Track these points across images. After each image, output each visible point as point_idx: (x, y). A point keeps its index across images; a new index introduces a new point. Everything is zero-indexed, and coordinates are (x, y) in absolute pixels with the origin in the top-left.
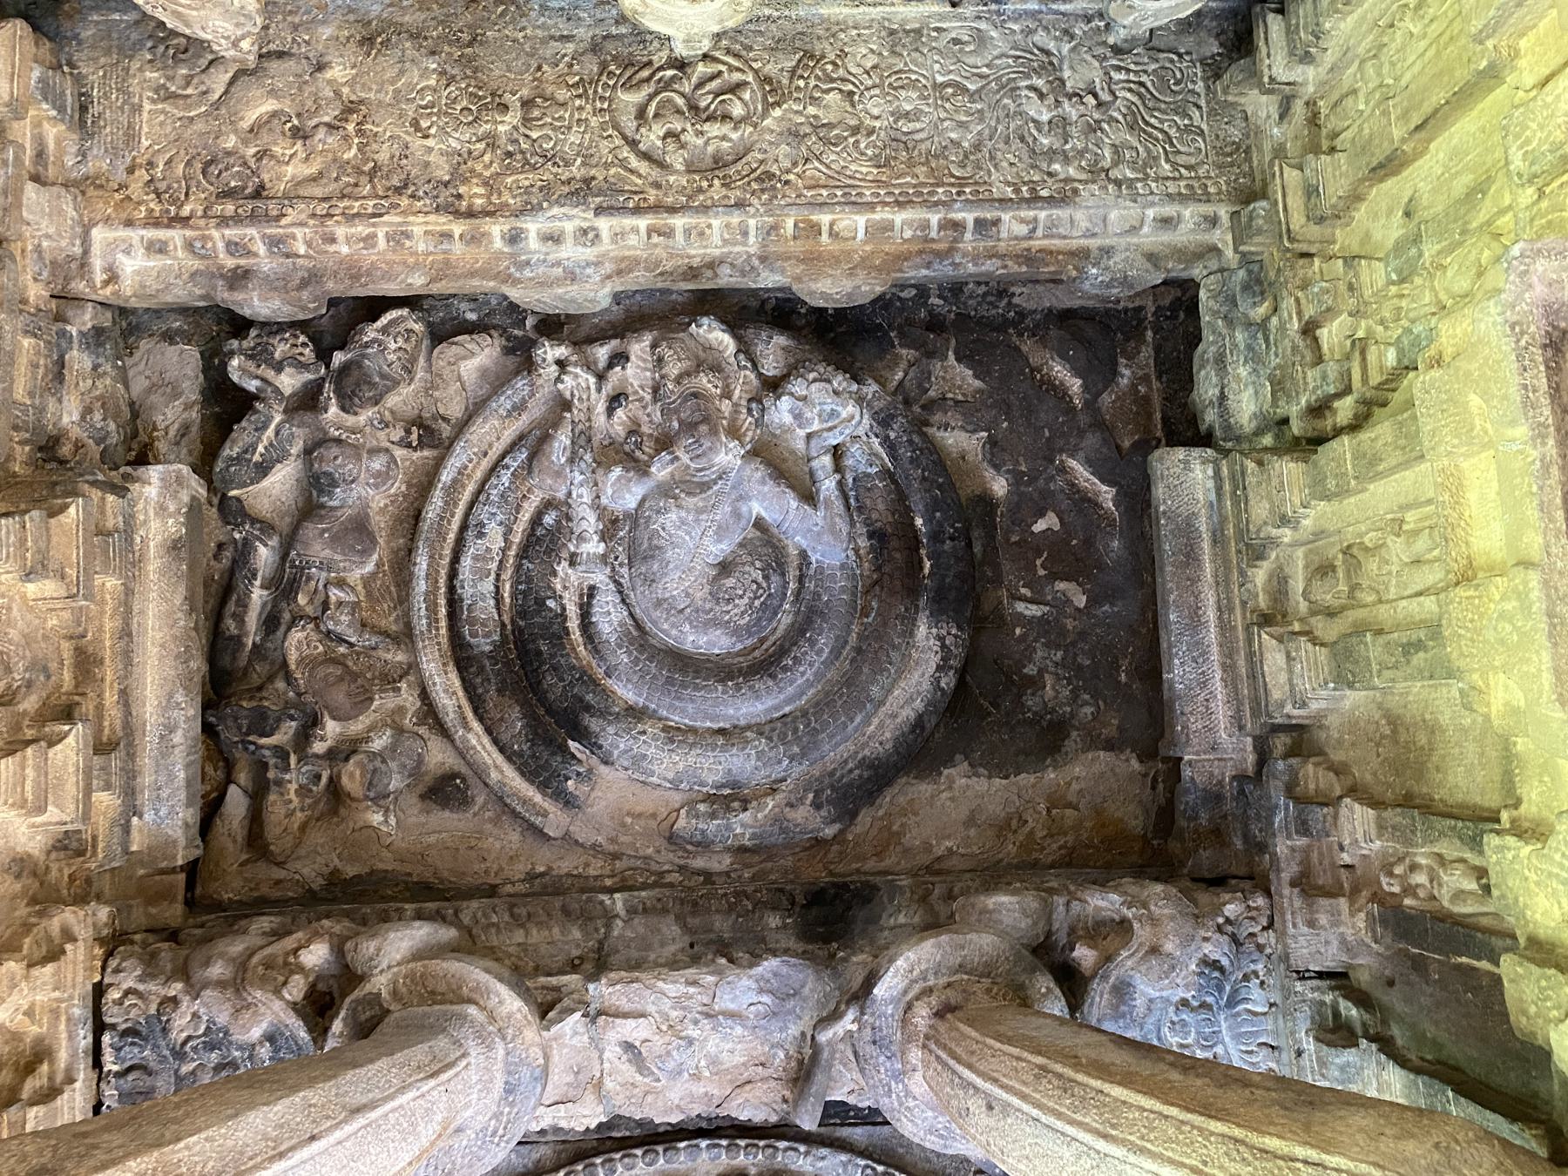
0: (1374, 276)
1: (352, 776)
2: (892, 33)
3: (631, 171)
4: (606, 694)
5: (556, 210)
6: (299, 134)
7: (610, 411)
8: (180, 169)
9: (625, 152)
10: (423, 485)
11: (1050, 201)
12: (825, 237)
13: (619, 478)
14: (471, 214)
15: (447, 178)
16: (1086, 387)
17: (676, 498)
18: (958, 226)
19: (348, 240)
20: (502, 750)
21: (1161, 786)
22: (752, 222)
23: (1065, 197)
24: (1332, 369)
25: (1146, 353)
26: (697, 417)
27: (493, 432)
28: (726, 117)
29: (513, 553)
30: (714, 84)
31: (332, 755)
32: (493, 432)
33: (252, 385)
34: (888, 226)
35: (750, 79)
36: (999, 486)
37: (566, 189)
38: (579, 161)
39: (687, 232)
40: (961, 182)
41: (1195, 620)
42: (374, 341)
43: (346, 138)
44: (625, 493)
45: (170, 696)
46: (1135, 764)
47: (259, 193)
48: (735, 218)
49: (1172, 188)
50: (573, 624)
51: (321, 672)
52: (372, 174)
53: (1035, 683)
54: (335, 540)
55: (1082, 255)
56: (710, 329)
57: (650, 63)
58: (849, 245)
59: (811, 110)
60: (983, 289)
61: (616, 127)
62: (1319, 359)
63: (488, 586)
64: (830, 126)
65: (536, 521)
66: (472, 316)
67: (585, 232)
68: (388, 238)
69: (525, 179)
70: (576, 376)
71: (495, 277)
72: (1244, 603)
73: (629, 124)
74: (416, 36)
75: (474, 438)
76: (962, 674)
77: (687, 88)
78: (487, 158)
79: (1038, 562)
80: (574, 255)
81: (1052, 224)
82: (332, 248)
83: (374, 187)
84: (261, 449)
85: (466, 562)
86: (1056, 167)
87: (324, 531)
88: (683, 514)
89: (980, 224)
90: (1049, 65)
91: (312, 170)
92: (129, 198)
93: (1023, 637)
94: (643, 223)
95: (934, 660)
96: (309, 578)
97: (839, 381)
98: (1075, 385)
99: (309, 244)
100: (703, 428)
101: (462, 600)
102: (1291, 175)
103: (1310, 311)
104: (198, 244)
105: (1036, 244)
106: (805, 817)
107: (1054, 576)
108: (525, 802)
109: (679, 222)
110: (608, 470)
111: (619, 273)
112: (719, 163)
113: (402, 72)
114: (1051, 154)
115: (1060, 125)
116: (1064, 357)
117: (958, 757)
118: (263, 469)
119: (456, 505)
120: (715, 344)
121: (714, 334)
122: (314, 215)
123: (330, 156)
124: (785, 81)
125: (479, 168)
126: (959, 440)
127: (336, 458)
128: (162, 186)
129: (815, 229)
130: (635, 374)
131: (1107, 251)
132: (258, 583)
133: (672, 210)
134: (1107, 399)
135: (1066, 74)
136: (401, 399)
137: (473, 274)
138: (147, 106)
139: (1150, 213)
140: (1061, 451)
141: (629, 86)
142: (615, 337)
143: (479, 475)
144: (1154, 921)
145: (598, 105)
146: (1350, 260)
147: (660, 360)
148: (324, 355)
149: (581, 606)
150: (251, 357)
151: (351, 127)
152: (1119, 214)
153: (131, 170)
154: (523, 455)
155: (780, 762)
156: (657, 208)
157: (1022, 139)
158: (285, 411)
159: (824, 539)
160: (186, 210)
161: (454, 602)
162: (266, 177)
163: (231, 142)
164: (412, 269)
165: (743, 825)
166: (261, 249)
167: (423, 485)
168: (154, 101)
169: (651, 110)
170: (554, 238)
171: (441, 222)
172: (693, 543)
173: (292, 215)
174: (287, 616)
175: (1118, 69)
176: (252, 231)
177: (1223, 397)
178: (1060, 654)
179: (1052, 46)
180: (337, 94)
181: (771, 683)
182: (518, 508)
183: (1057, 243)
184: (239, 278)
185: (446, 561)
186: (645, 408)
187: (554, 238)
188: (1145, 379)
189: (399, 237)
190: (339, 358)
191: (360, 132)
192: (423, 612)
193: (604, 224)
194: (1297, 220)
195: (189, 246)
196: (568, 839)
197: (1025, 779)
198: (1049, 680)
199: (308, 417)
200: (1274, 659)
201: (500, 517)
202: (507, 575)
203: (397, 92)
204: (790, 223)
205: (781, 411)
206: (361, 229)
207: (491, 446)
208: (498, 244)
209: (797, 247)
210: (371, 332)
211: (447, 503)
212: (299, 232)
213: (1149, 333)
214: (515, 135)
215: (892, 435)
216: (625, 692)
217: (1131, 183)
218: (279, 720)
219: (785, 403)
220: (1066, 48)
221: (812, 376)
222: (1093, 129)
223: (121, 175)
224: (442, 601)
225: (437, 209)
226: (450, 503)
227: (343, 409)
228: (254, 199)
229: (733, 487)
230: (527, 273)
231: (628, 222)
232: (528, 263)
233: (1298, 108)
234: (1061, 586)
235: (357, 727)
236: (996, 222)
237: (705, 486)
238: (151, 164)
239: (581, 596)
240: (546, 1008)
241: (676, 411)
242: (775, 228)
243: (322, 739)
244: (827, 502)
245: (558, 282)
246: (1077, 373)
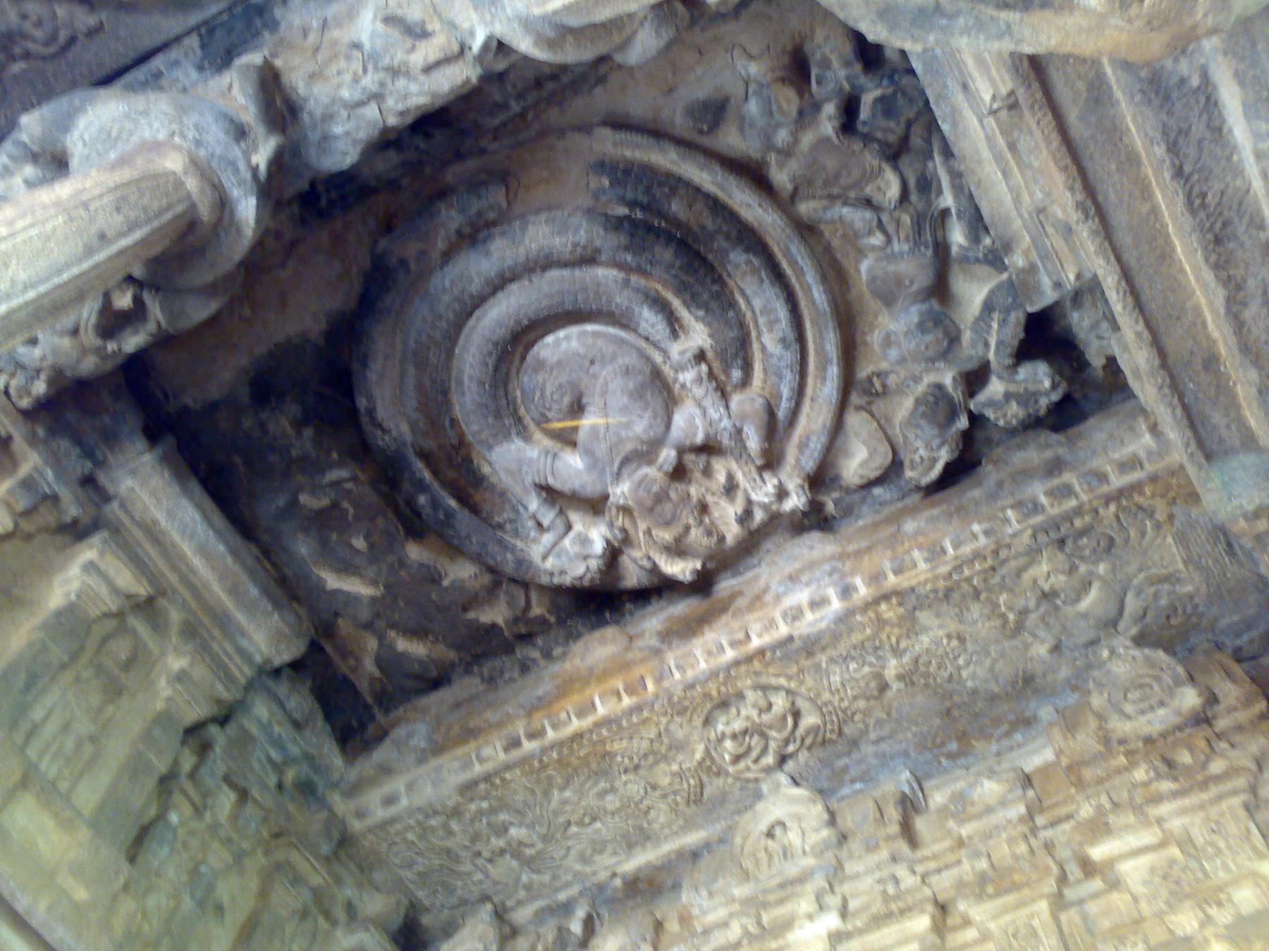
0: (218, 857)
1: (789, 101)
2: (648, 838)
3: (778, 675)
4: (620, 266)
5: (823, 625)
6: (1047, 596)
7: (730, 477)
8: (1132, 533)
9: (793, 685)
10: (849, 352)
11: (475, 783)
12: (621, 687)
13: (695, 434)
14: (886, 597)
15: (918, 613)
16: (392, 647)
17: (643, 442)
18: (532, 736)
19: (975, 536)
20: (679, 179)
21: (162, 397)
22: (677, 675)
23: (468, 789)
24: (210, 782)
25: (364, 687)
26: (658, 509)
27: (813, 420)
28: (734, 737)
29: (754, 334)
30: (754, 754)
31: (817, 107)
32: (813, 420)
33: (1024, 371)
34: (581, 714)
35: (731, 769)
36: (415, 552)
37: (823, 642)
38: (824, 665)
39: (721, 649)
40: (544, 767)
41: (203, 551)
42: (939, 447)
43: (1011, 608)
44: (690, 421)
45: (955, 124)
46: (188, 400)
47: (1062, 542)
48: (690, 674)
49: (398, 826)
50: (676, 303)
51: (856, 174)
52: (977, 594)
53: (299, 425)
54: (899, 281)
55: (437, 749)
56: (683, 572)
57: (809, 748)
58: (604, 686)
59: (675, 767)
60: (507, 676)
61: (810, 699)
62: (227, 779)
63: (758, 303)
64: (656, 763)
65: (747, 368)
66: (877, 491)
67: (795, 618)
68: (944, 551)
69: (856, 638)
70: (766, 494)
71: (848, 556)
72: (175, 591)
73: (802, 704)
74: (993, 698)
75: (825, 408)
76: (355, 411)
77: (773, 745)
78: (894, 640)
79: (351, 511)
80: (798, 594)
81: (467, 765)
82: (986, 525)
83: (971, 585)
84: (995, 325)
85: (782, 313)
86: (485, 805)
87: (912, 282)
88: (631, 434)
89: (516, 743)
90: (529, 864)
91: (1027, 577)
92: (1163, 496)
93: (329, 452)
94: (756, 642)
95: (381, 413)
96: (907, 239)
97: (567, 580)
98: (402, 645)
99: (1007, 520)
100: (649, 503)
101: (772, 284)
102: (316, 880)
103: (249, 809)
104: (1095, 483)
105: (473, 745)
106: (411, 249)
107: (335, 505)
108: (637, 146)
109: (730, 654)
110: (707, 436)
111: (758, 598)
112: (724, 705)
113: (991, 669)
114: (493, 811)
115: (503, 830)
116: (420, 662)
117: (321, 342)
118: (988, 307)
119: (816, 352)
120: (677, 560)
121: (681, 569)
122: (1009, 546)
123: (1017, 590)
124: (705, 778)
125: (896, 631)
126: (462, 572)
127: (927, 348)
128: (1140, 515)
129: (630, 691)
130: (727, 515)
131: (421, 760)
132: (953, 211)
133: (737, 663)
134: (372, 644)
135: (515, 864)
136: (903, 407)
137: (869, 549)
138: (1181, 566)
139: (404, 802)
140: (383, 597)
141: (815, 730)
142: (758, 531)
143: (810, 381)
144: (84, 351)
145: (830, 708)
146: (239, 857)
147: (709, 534)
148: (976, 420)
149: (678, 320)
150: (1034, 394)
151: (1011, 617)
152: (427, 793)
153: (1171, 517)
154: (782, 413)
155: (452, 282)
156: (749, 659)
157: (518, 812)
158: (988, 363)
159: (514, 461)
160: (1112, 508)
161: (778, 276)
162: (1061, 556)
163: (1102, 568)
164: (918, 532)
165: (451, 218)
166: (1043, 499)
167: (849, 352)
168: (1178, 571)
169: (790, 721)
170: (816, 604)
171: (904, 581)
172: (611, 417)
173: (1026, 538)
174: (914, 197)
175: (481, 882)
176: (1055, 511)
177: (282, 706)
178: (294, 453)
179: (534, 876)
180: (1035, 636)
181: (494, 338)
182: (765, 371)
183: (460, 751)
184: (1055, 467)
185: (803, 303)
186: (707, 490)
187: (816, 604)
188: (354, 670)
189: (935, 553)
190: (963, 423)
191: (1003, 616)
192: (799, 259)
193: (783, 630)
194: (295, 857)
195: (1103, 478)
196: (585, 128)
197: (261, 349)
198: (290, 430)
199: (969, 366)
200: (126, 579)
201: (774, 360)
202: (749, 315)
203: (988, 654)
204: (651, 686)
205: (597, 536)
206: (967, 549)
207: (811, 408)
208: (858, 581)
209: (639, 671)
210: (944, 456)
211: (823, 349)
212: (1016, 526)
213: (370, 700)
214: (881, 663)
215: (509, 556)
216: (604, 274)
217: (427, 816)
218: (874, 116)
219: (598, 547)
220: (524, 878)
221: (589, 576)
222: (475, 838)
223: (1177, 510)
224: (789, 271)
225: (913, 589)
226: (821, 351)
227: (939, 387)
228: (1060, 537)
229: (603, 471)
230: (827, 567)
231: (767, 639)
232: (830, 574)
233: (341, 915)
234: (325, 502)
235: (807, 139)
236: (506, 750)
237: (626, 461)
238: (1158, 526)
239: (682, 327)
240: (501, 47)
241: (676, 506)
242: (659, 680)
243: (830, 118)
244: (526, 490)
245: (801, 571)
246: (404, 656)
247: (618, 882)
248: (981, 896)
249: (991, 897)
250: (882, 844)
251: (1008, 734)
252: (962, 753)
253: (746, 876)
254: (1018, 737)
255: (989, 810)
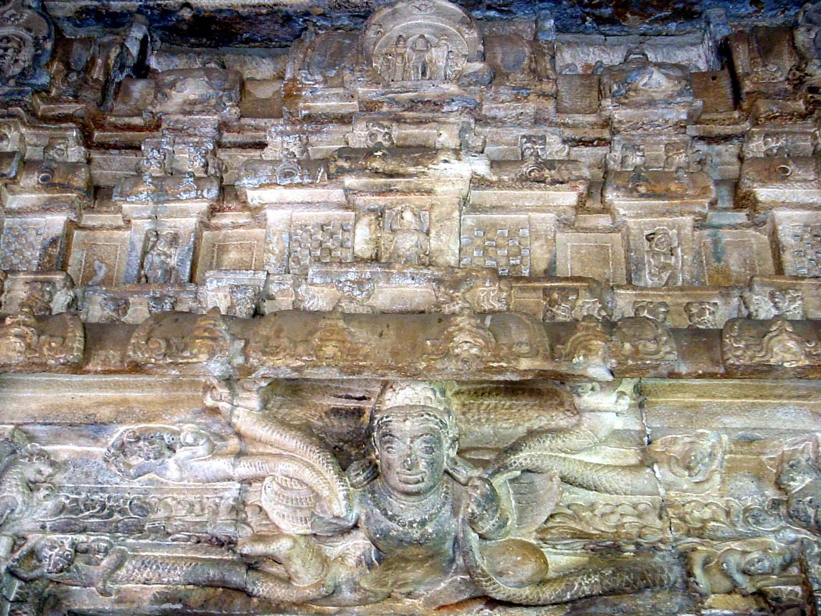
247: (187, 14)
248: (632, 192)
249: (642, 196)
250: (532, 97)
251: (665, 20)
252: (611, 21)
253: (376, 79)
254: (673, 26)
255: (652, 103)
